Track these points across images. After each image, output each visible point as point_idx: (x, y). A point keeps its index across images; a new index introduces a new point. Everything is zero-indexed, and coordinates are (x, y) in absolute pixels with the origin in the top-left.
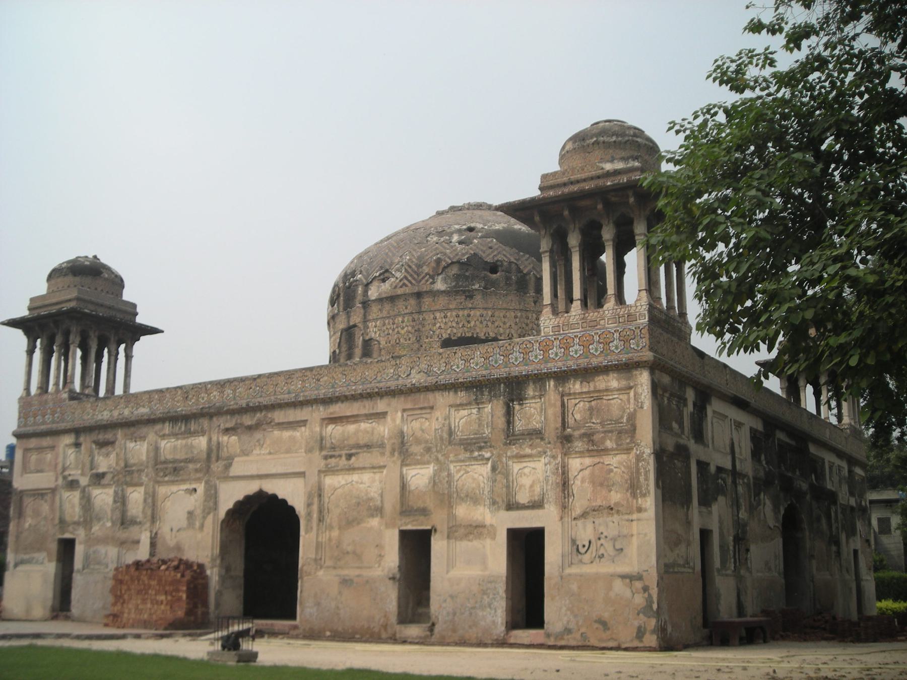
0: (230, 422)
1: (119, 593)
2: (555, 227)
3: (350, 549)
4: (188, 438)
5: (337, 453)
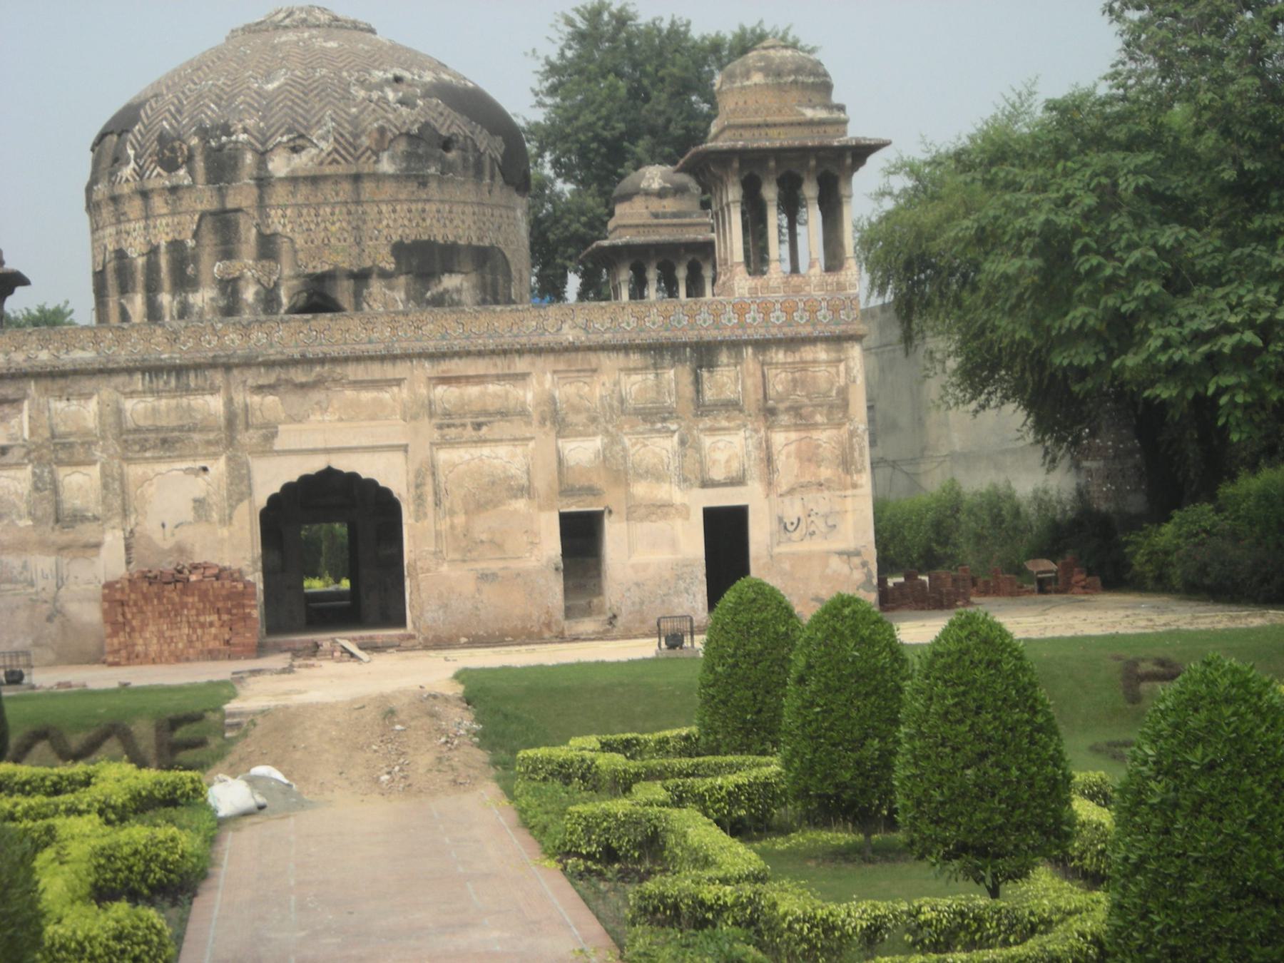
0: (270, 377)
1: (120, 619)
2: (746, 173)
3: (484, 537)
4: (181, 396)
5: (457, 422)
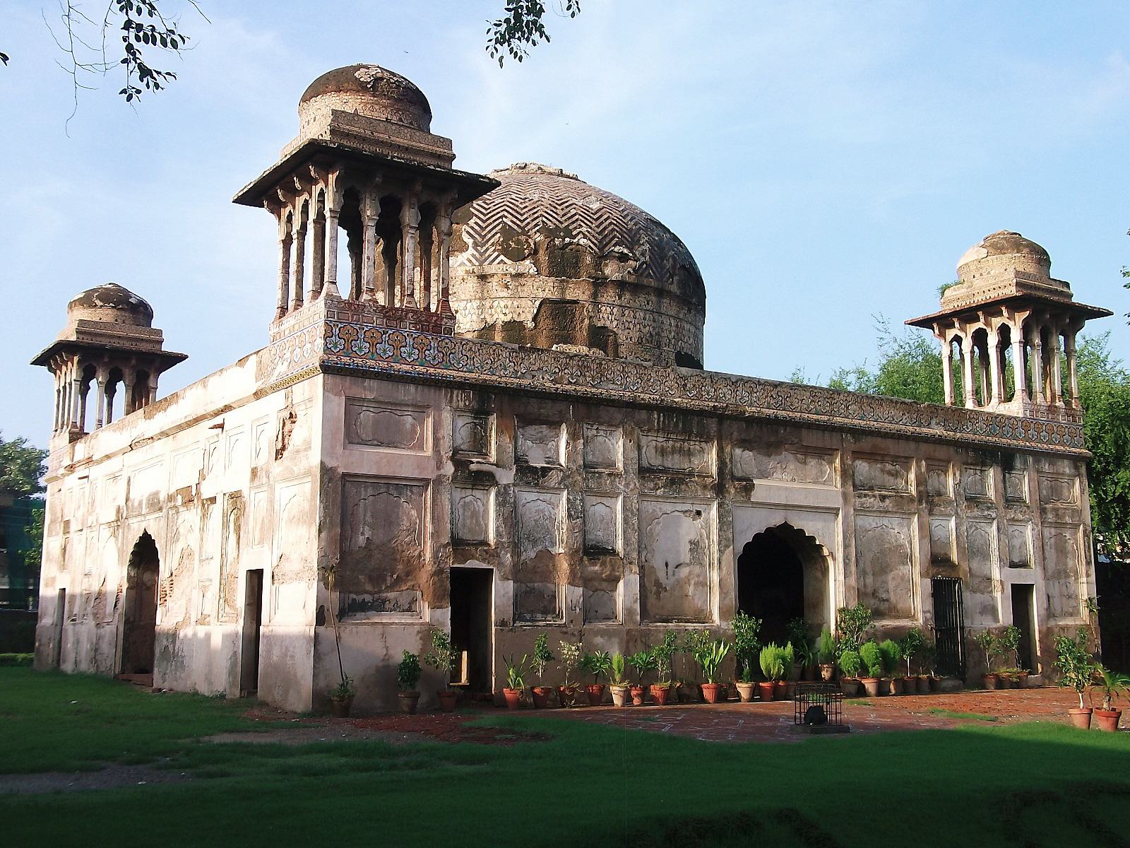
4: (684, 441)
